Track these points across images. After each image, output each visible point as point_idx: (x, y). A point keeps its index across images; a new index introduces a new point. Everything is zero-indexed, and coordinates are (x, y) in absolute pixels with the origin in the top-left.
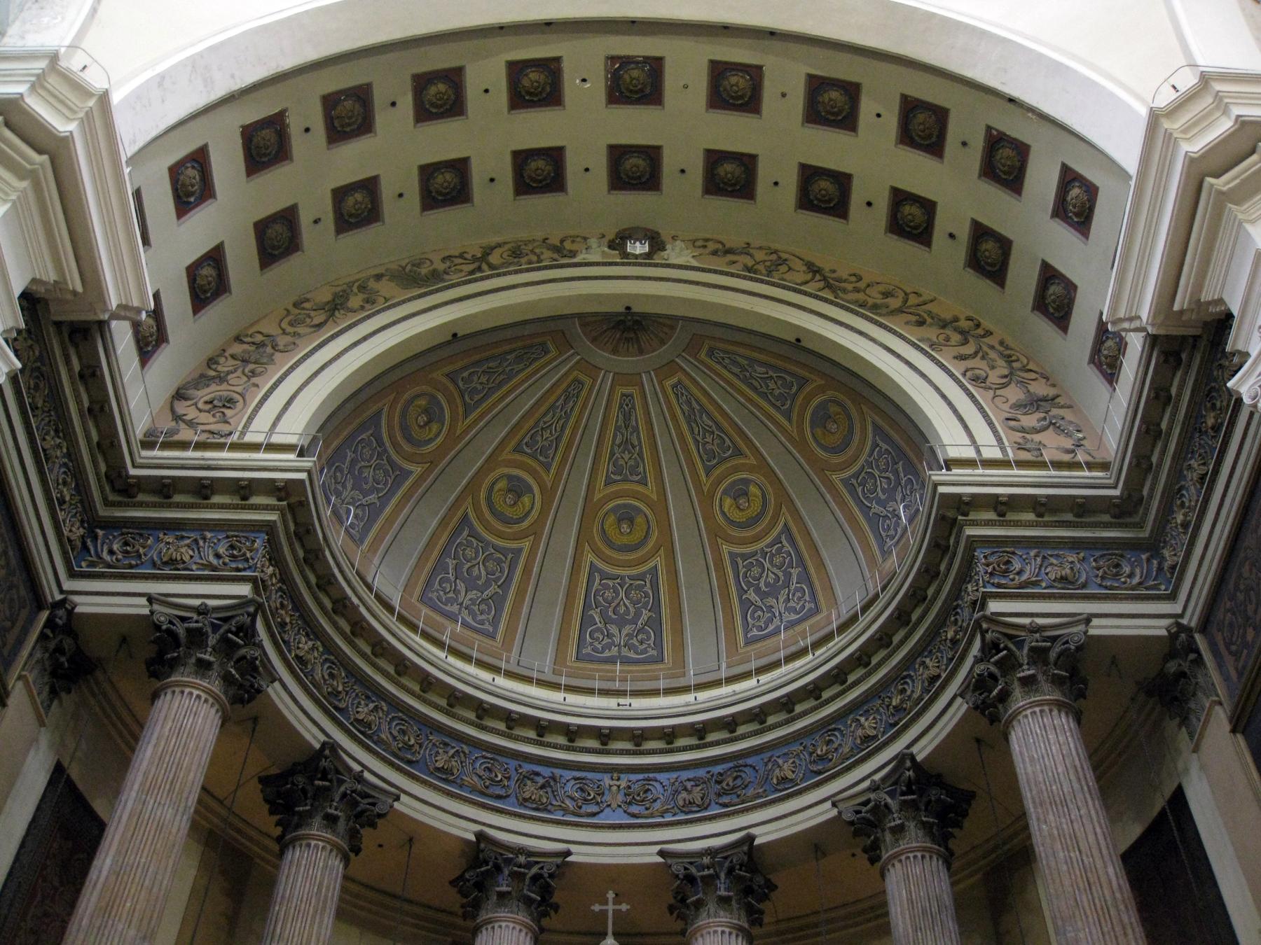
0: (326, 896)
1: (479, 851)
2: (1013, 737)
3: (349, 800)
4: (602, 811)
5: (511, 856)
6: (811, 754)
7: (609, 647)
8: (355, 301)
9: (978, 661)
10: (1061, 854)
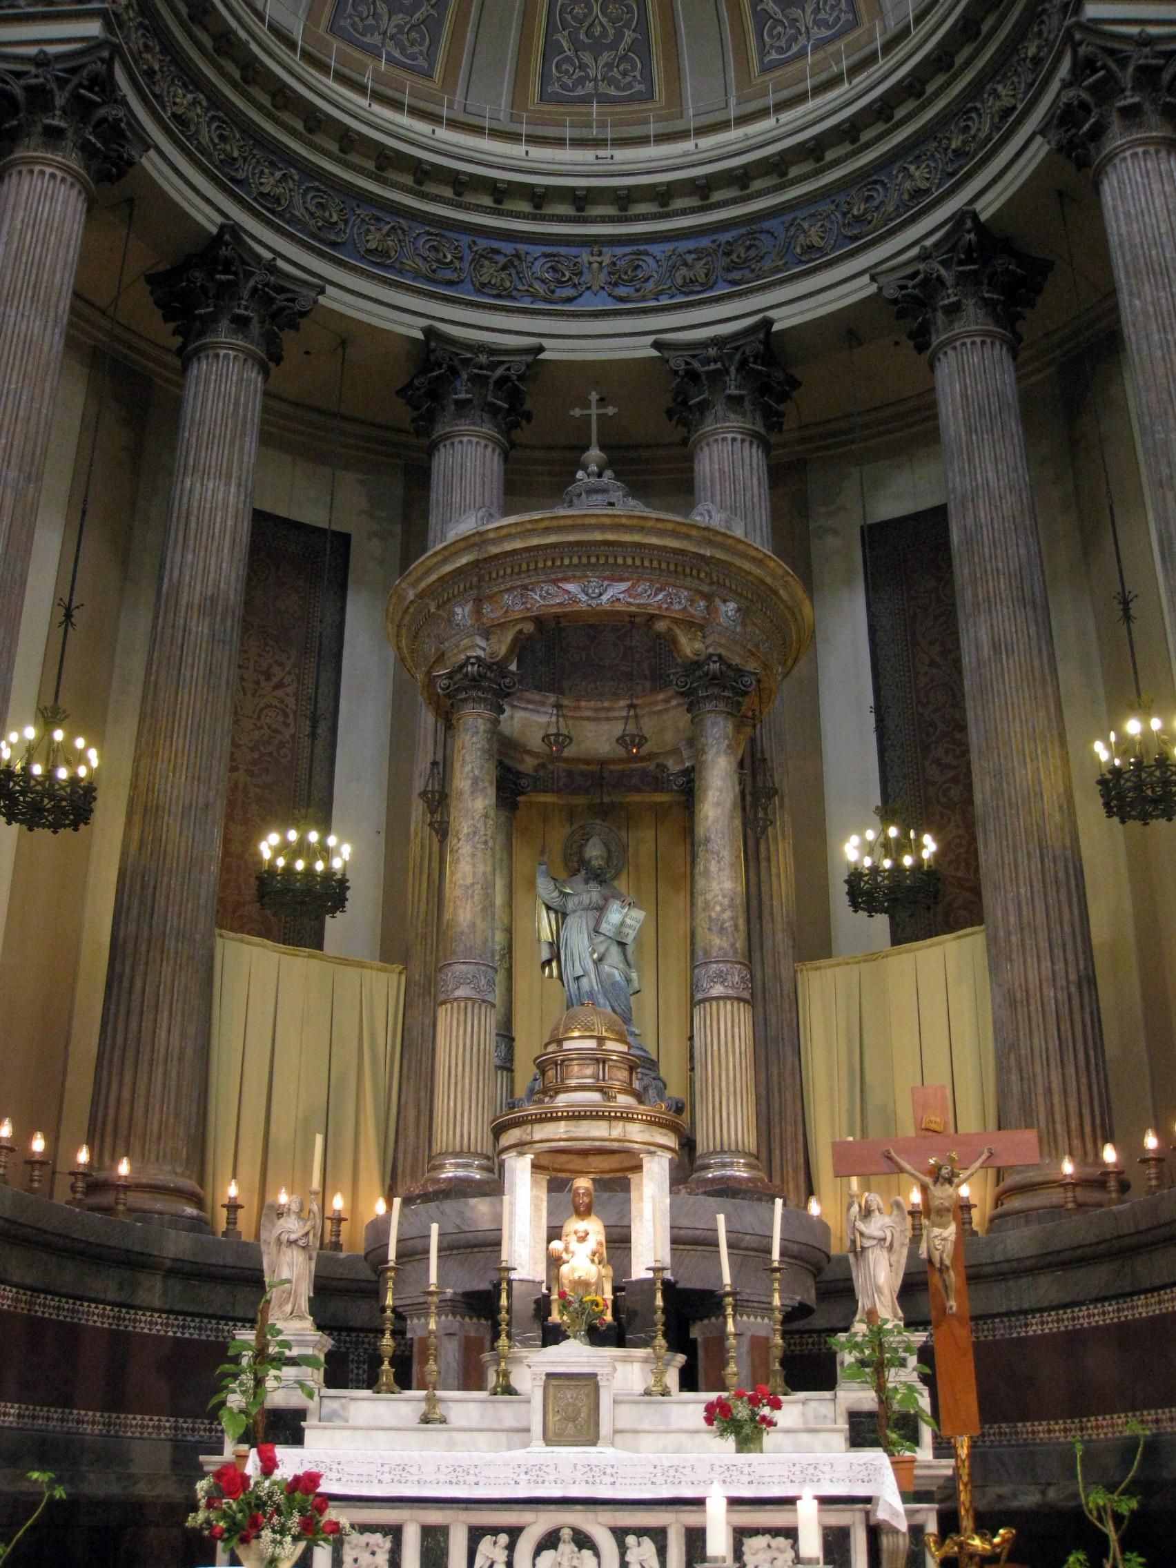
0: (245, 416)
1: (431, 351)
2: (1106, 187)
3: (261, 297)
4: (580, 295)
5: (469, 356)
6: (845, 214)
7: (581, 81)
9: (1066, 85)
10: (1156, 337)
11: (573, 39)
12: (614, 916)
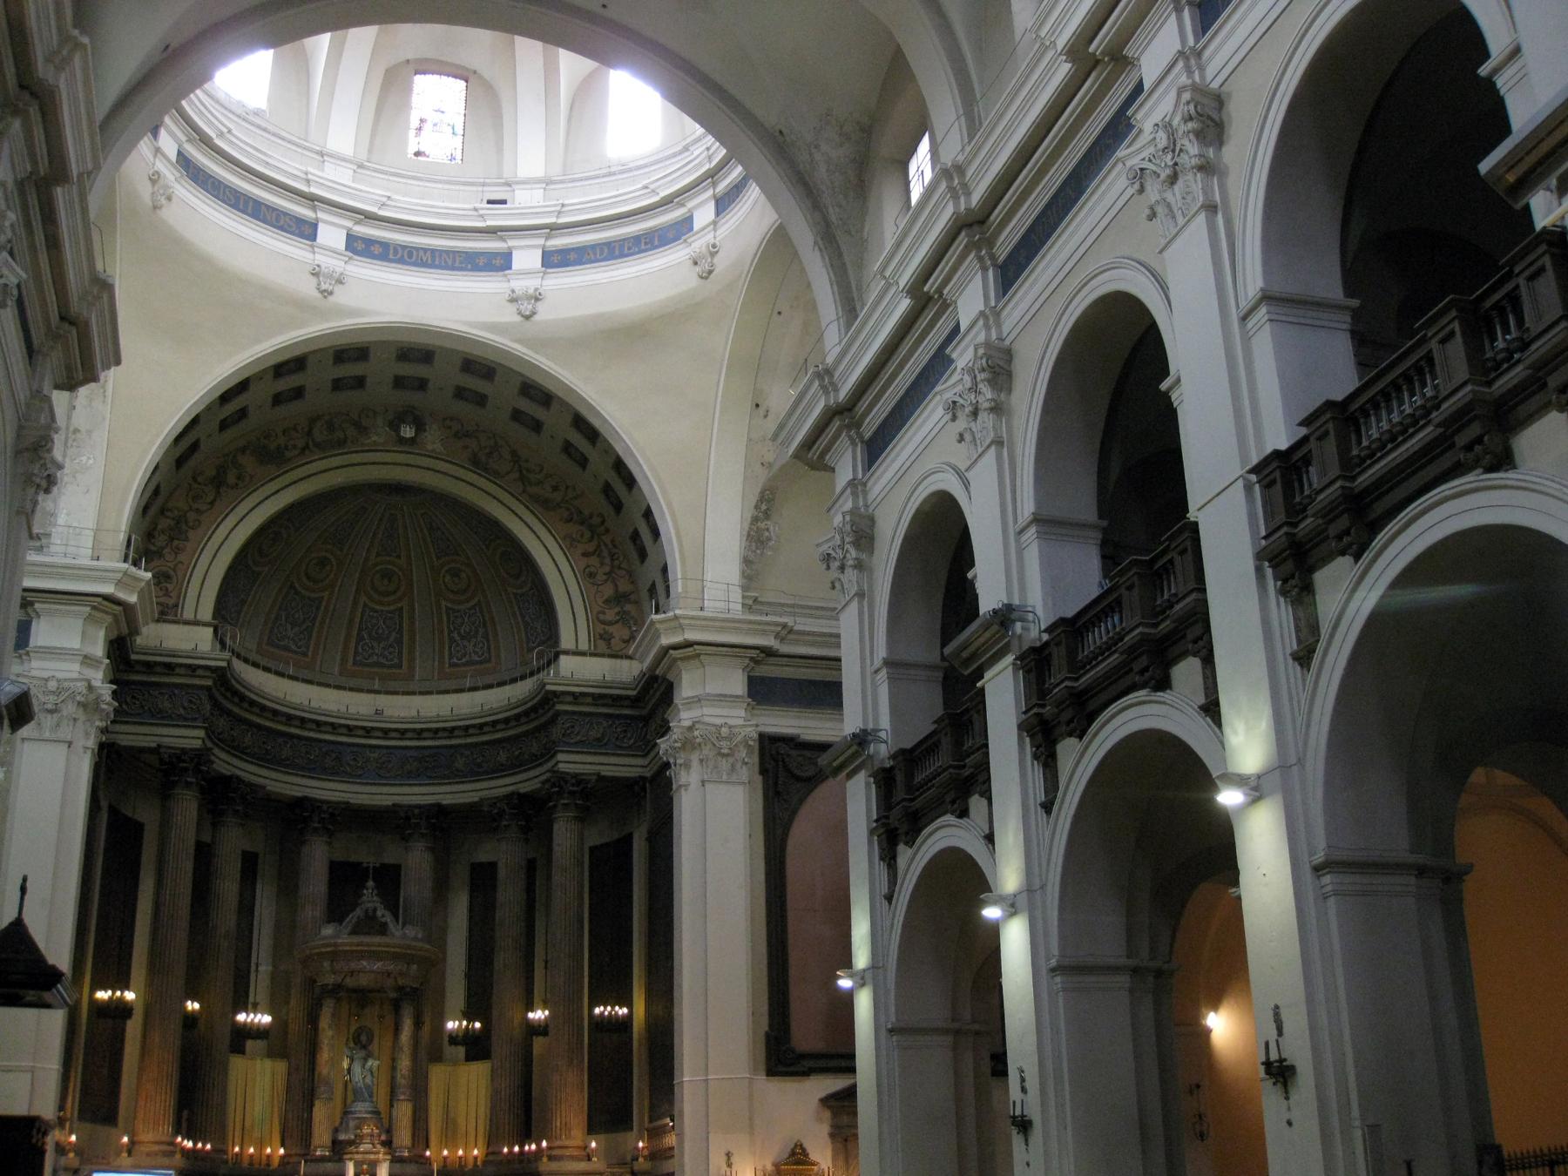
8: (231, 479)
12: (370, 1063)
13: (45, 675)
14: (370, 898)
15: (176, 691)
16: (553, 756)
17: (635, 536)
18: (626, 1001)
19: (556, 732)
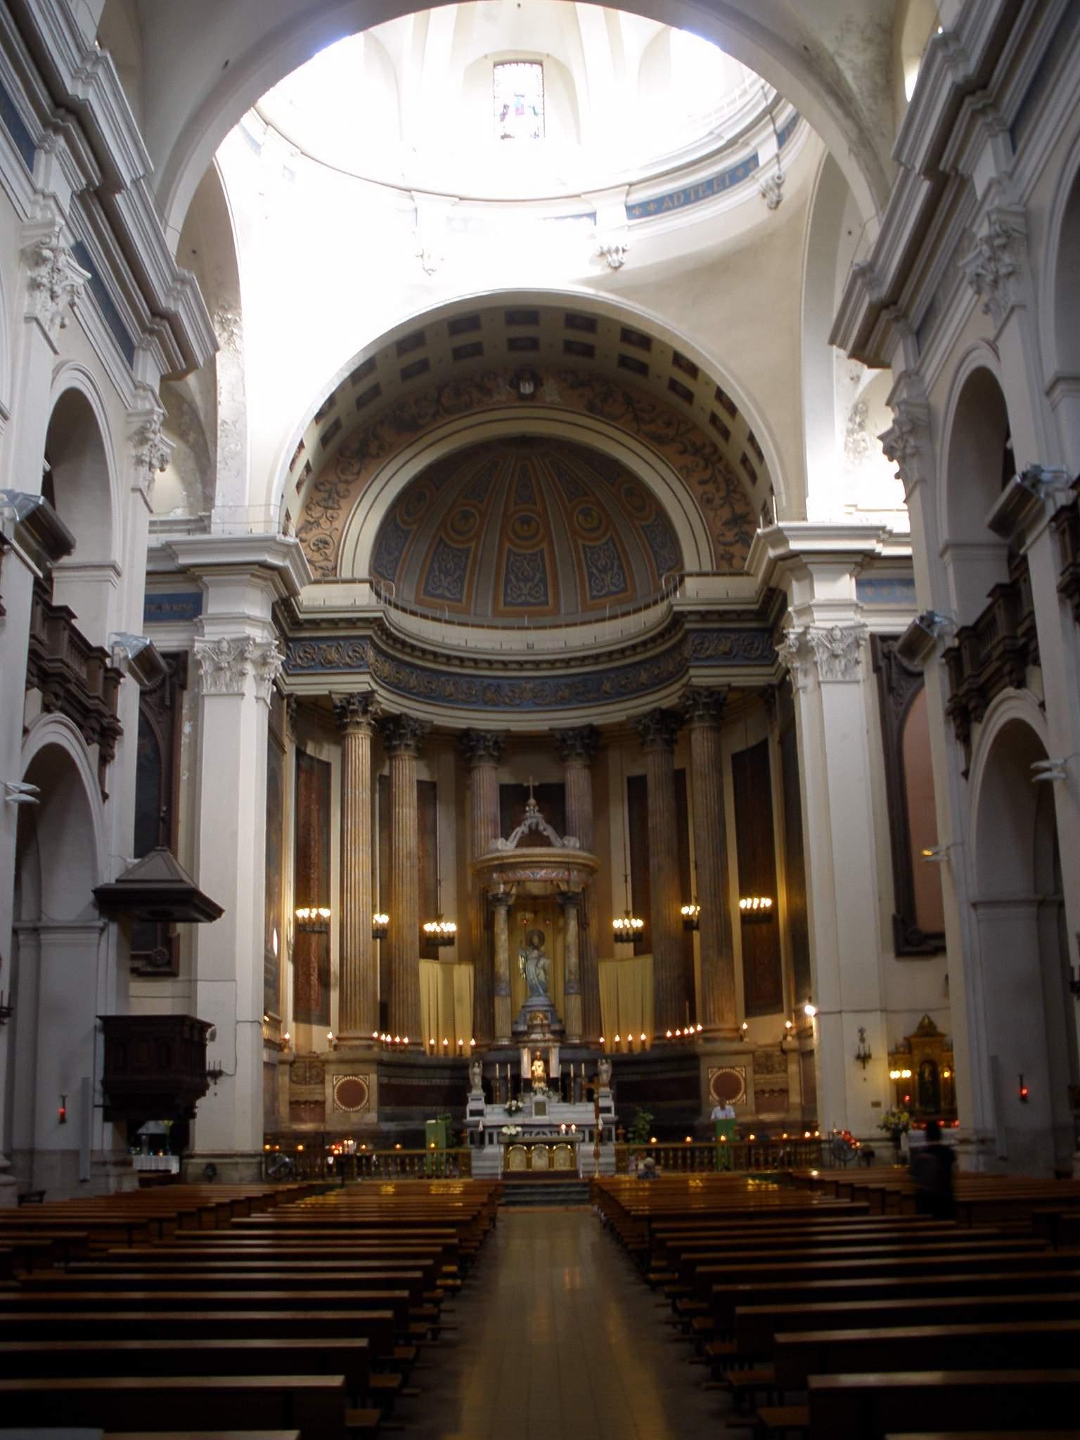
7: (519, 596)
8: (373, 449)
11: (516, 577)
12: (542, 962)
13: (216, 638)
14: (533, 815)
15: (342, 643)
16: (687, 671)
17: (745, 460)
18: (771, 892)
19: (687, 650)
